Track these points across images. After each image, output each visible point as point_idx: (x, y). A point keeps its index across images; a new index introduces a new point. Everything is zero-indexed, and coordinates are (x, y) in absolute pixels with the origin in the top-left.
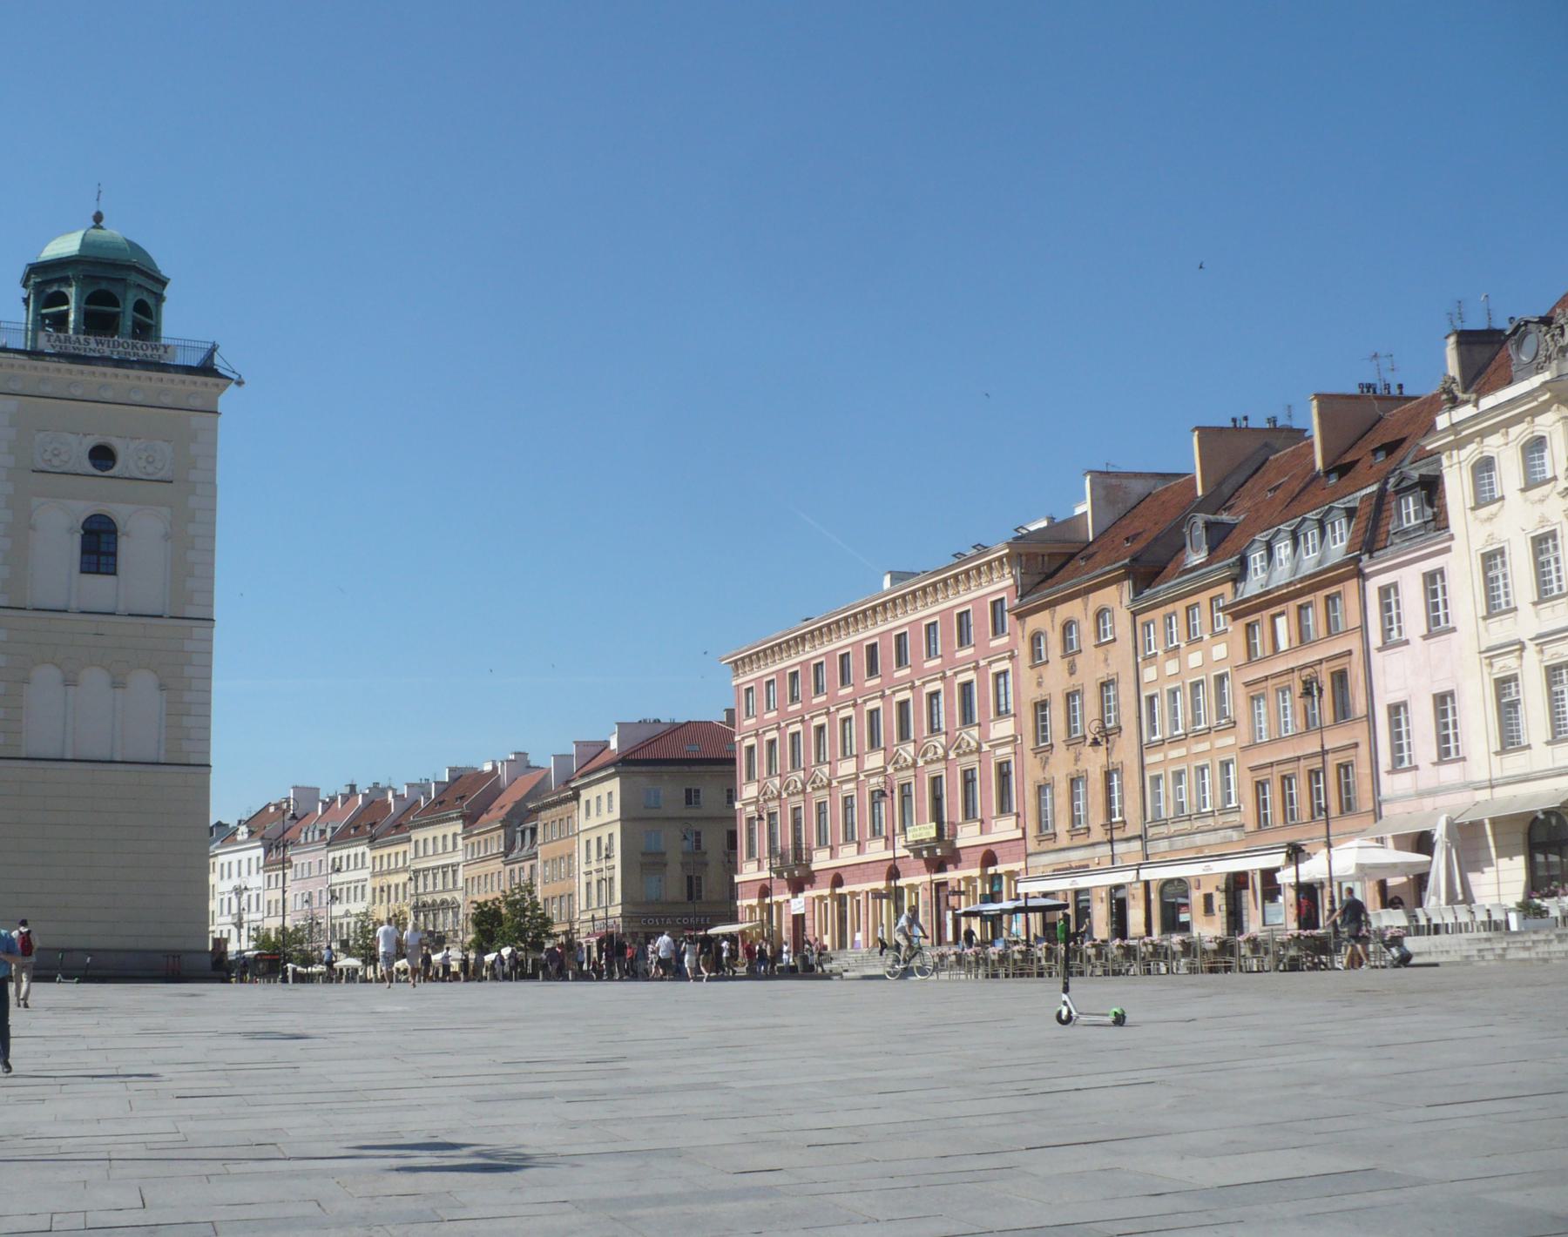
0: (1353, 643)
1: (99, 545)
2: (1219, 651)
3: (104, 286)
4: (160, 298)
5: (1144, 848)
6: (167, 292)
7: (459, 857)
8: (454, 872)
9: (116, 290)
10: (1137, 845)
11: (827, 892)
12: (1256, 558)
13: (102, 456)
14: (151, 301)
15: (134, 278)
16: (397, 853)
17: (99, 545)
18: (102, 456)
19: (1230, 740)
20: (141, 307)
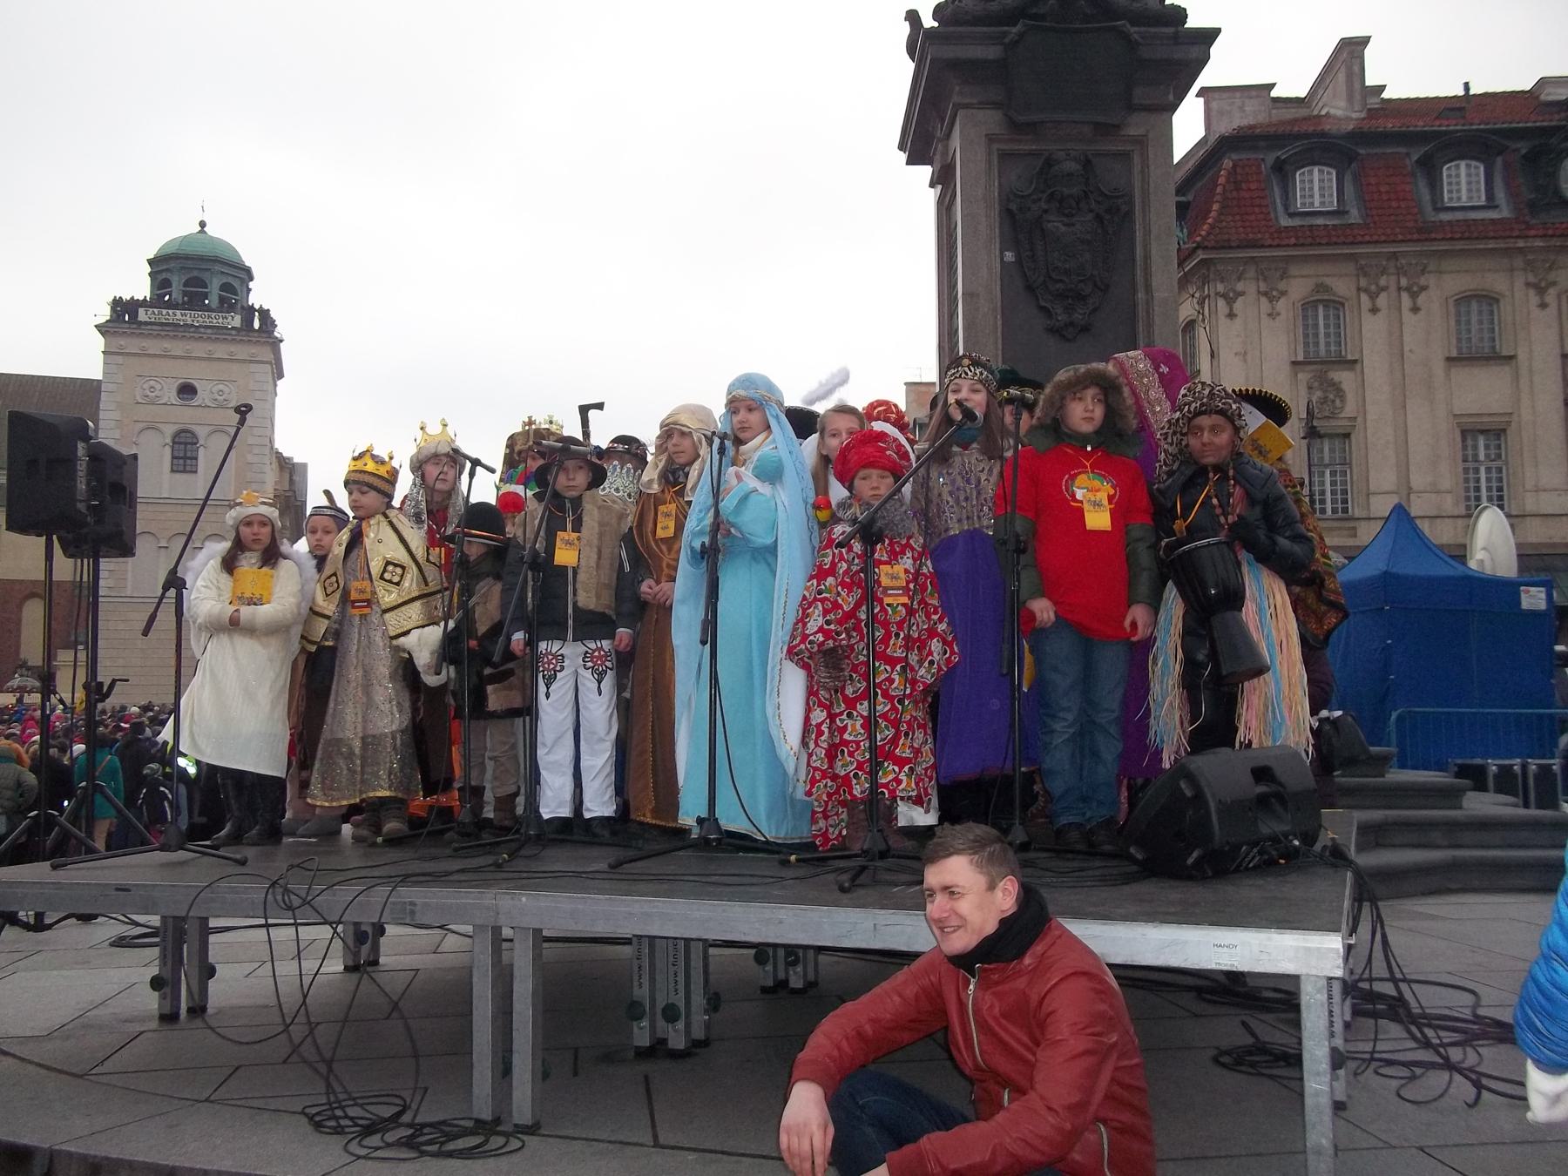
3: (195, 273)
9: (205, 276)
13: (187, 390)
14: (236, 284)
15: (218, 267)
18: (187, 390)
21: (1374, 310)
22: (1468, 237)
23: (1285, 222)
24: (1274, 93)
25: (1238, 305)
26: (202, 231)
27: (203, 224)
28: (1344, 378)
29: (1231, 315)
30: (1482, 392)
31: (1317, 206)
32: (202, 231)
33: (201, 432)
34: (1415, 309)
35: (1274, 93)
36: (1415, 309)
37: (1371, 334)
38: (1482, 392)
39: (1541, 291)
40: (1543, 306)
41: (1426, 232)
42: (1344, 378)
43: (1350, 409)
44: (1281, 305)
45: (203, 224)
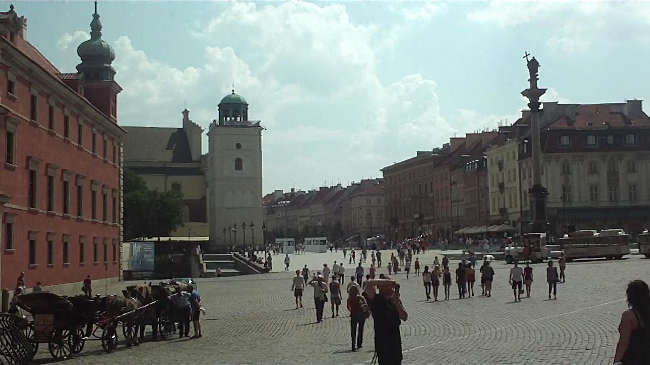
0: (477, 188)
1: (239, 164)
2: (462, 185)
4: (247, 109)
5: (452, 223)
6: (248, 107)
7: (323, 213)
8: (322, 217)
10: (450, 222)
11: (401, 228)
12: (467, 167)
13: (238, 146)
16: (306, 211)
17: (239, 164)
19: (463, 203)
20: (244, 112)
21: (575, 164)
22: (592, 150)
23: (559, 148)
24: (558, 103)
25: (551, 162)
26: (233, 94)
27: (233, 91)
28: (570, 177)
29: (550, 165)
30: (593, 179)
31: (565, 144)
32: (233, 94)
33: (242, 158)
34: (582, 164)
35: (558, 103)
36: (582, 164)
37: (574, 169)
38: (593, 179)
39: (604, 161)
40: (604, 164)
41: (584, 150)
42: (570, 177)
43: (571, 182)
44: (559, 163)
45: (233, 91)
